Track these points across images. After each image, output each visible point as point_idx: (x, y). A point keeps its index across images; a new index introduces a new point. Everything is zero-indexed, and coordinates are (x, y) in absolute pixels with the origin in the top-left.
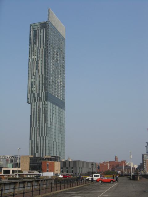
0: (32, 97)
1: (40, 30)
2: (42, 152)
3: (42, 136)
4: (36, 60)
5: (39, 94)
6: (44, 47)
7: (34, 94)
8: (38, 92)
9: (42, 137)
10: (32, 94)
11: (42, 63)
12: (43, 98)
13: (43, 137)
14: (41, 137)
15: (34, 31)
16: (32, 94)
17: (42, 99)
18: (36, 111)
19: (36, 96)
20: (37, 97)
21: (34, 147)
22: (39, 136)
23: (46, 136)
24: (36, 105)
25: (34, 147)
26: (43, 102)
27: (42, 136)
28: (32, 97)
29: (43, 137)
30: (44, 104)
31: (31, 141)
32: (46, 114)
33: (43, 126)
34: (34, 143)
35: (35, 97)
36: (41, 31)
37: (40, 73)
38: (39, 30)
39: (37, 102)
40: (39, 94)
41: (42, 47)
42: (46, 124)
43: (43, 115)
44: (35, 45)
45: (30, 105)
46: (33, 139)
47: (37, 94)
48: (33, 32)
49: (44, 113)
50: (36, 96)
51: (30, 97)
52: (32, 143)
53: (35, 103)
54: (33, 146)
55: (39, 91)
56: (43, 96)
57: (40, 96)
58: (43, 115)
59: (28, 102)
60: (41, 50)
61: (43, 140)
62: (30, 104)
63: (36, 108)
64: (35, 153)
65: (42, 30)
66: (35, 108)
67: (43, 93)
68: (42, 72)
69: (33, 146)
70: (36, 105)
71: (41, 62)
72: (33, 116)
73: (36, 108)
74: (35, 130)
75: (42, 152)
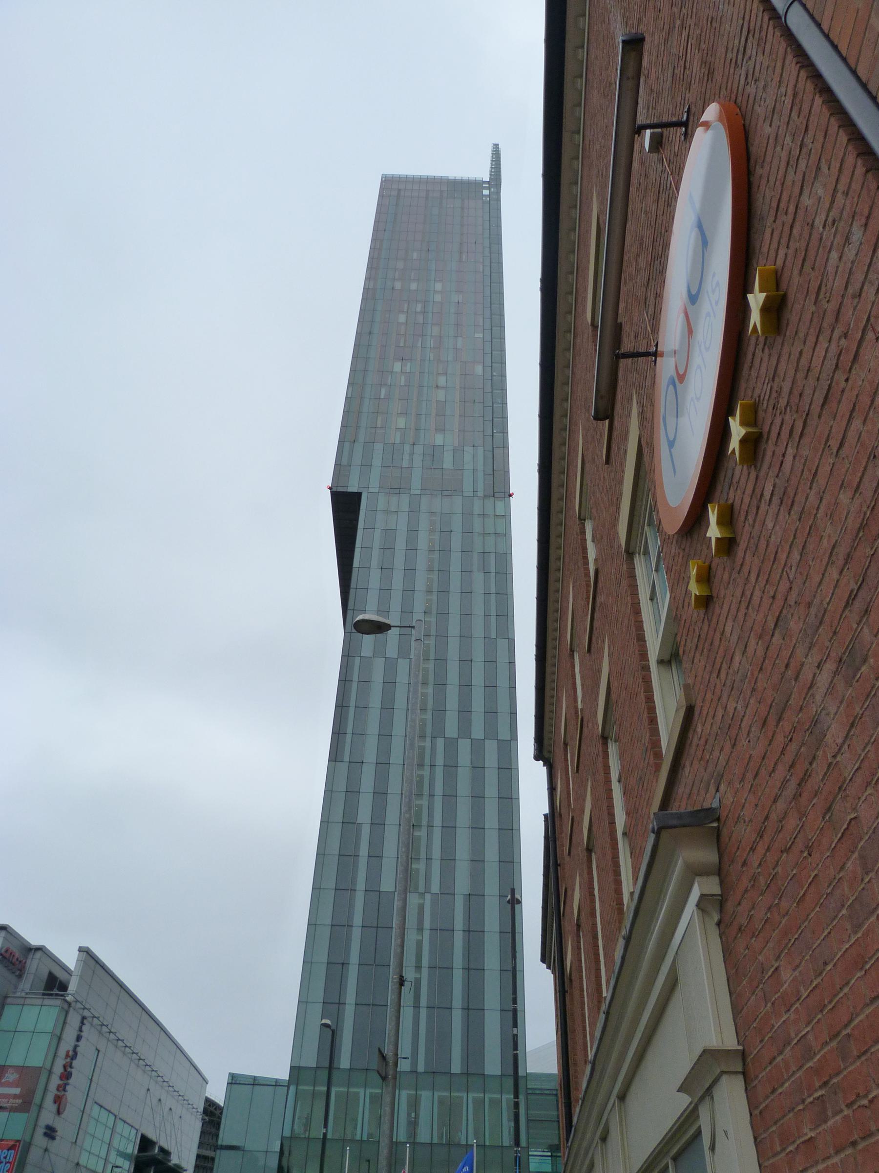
2: (462, 885)
3: (465, 729)
9: (464, 746)
10: (379, 447)
13: (478, 748)
14: (451, 746)
18: (411, 548)
20: (418, 462)
21: (378, 823)
22: (439, 730)
23: (504, 735)
24: (414, 512)
25: (378, 823)
27: (465, 729)
28: (377, 461)
29: (478, 748)
30: (477, 510)
31: (343, 768)
33: (478, 655)
34: (380, 794)
42: (502, 644)
43: (478, 577)
46: (370, 755)
47: (419, 449)
52: (352, 793)
53: (405, 499)
54: (364, 815)
57: (448, 463)
58: (478, 577)
61: (478, 768)
63: (412, 531)
64: (388, 884)
66: (402, 526)
67: (469, 450)
69: (364, 815)
70: (414, 512)
73: (412, 531)
74: (389, 684)
75: (462, 885)
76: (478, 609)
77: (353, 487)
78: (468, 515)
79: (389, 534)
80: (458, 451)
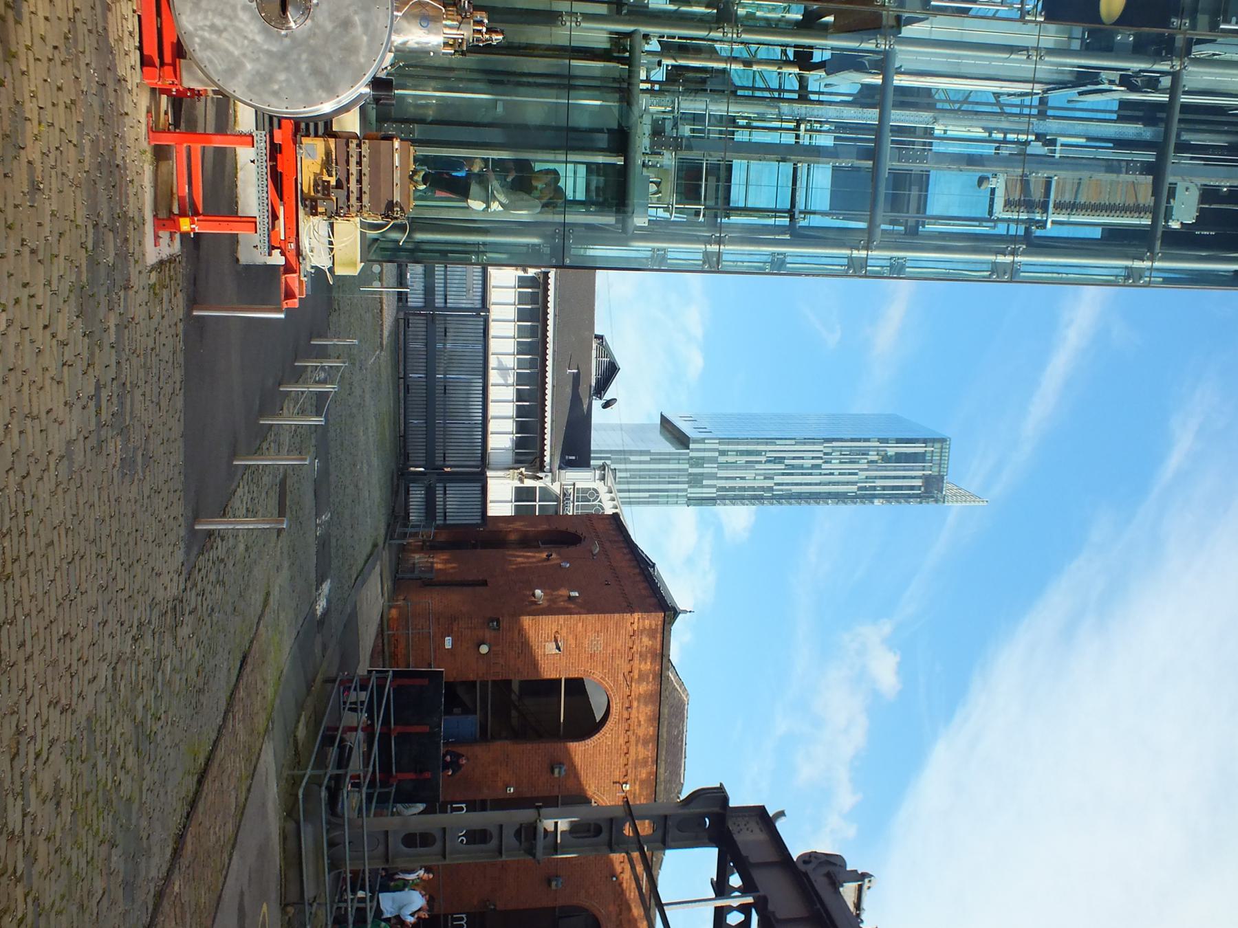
1: (920, 473)
4: (824, 466)
5: (713, 476)
6: (860, 489)
8: (721, 473)
10: (717, 454)
15: (924, 454)
19: (708, 469)
20: (705, 471)
26: (685, 490)
36: (920, 477)
37: (778, 479)
40: (713, 476)
49: (650, 497)
50: (708, 469)
55: (721, 478)
56: (705, 490)
57: (705, 482)
58: (647, 494)
65: (918, 483)
67: (714, 490)
72: (647, 458)
76: (632, 494)
77: (691, 446)
80: (714, 486)
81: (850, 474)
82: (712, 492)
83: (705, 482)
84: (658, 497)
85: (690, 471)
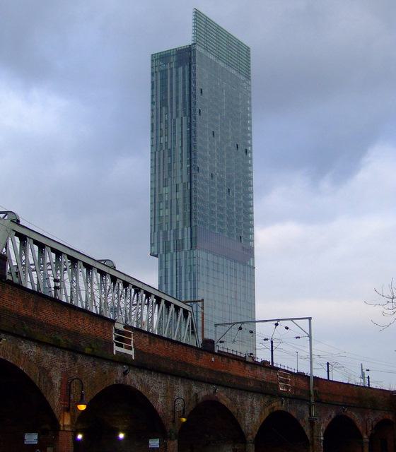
0: (161, 240)
4: (169, 147)
7: (165, 234)
10: (161, 233)
11: (182, 154)
12: (186, 240)
15: (160, 71)
16: (161, 233)
17: (183, 244)
18: (172, 275)
26: (186, 253)
32: (194, 280)
35: (169, 239)
37: (179, 181)
38: (171, 69)
39: (172, 251)
41: (181, 114)
44: (164, 108)
45: (156, 260)
47: (172, 231)
48: (159, 74)
50: (171, 238)
51: (156, 241)
53: (169, 254)
56: (186, 237)
57: (180, 238)
59: (152, 255)
60: (178, 121)
62: (157, 256)
65: (181, 69)
66: (169, 266)
67: (186, 229)
68: (182, 176)
70: (172, 260)
71: (180, 152)
78: (186, 257)
79: (166, 269)
80: (183, 230)
81: (175, 127)
82: (187, 230)
83: (180, 238)
84: (190, 274)
85: (172, 251)
